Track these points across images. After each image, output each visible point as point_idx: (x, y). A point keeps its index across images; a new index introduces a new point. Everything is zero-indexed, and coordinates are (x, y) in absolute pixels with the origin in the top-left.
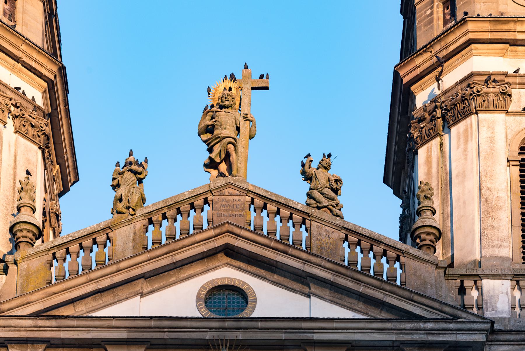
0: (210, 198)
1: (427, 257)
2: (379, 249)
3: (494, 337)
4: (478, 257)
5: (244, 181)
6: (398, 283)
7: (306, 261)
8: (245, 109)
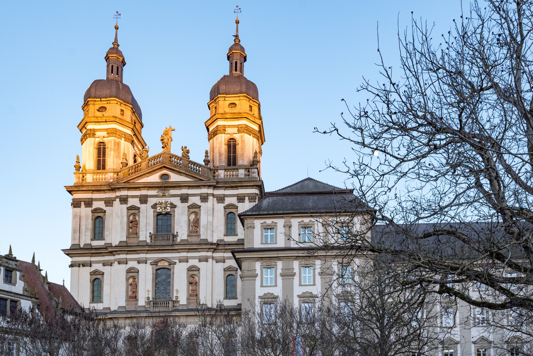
2: (196, 165)
8: (170, 135)
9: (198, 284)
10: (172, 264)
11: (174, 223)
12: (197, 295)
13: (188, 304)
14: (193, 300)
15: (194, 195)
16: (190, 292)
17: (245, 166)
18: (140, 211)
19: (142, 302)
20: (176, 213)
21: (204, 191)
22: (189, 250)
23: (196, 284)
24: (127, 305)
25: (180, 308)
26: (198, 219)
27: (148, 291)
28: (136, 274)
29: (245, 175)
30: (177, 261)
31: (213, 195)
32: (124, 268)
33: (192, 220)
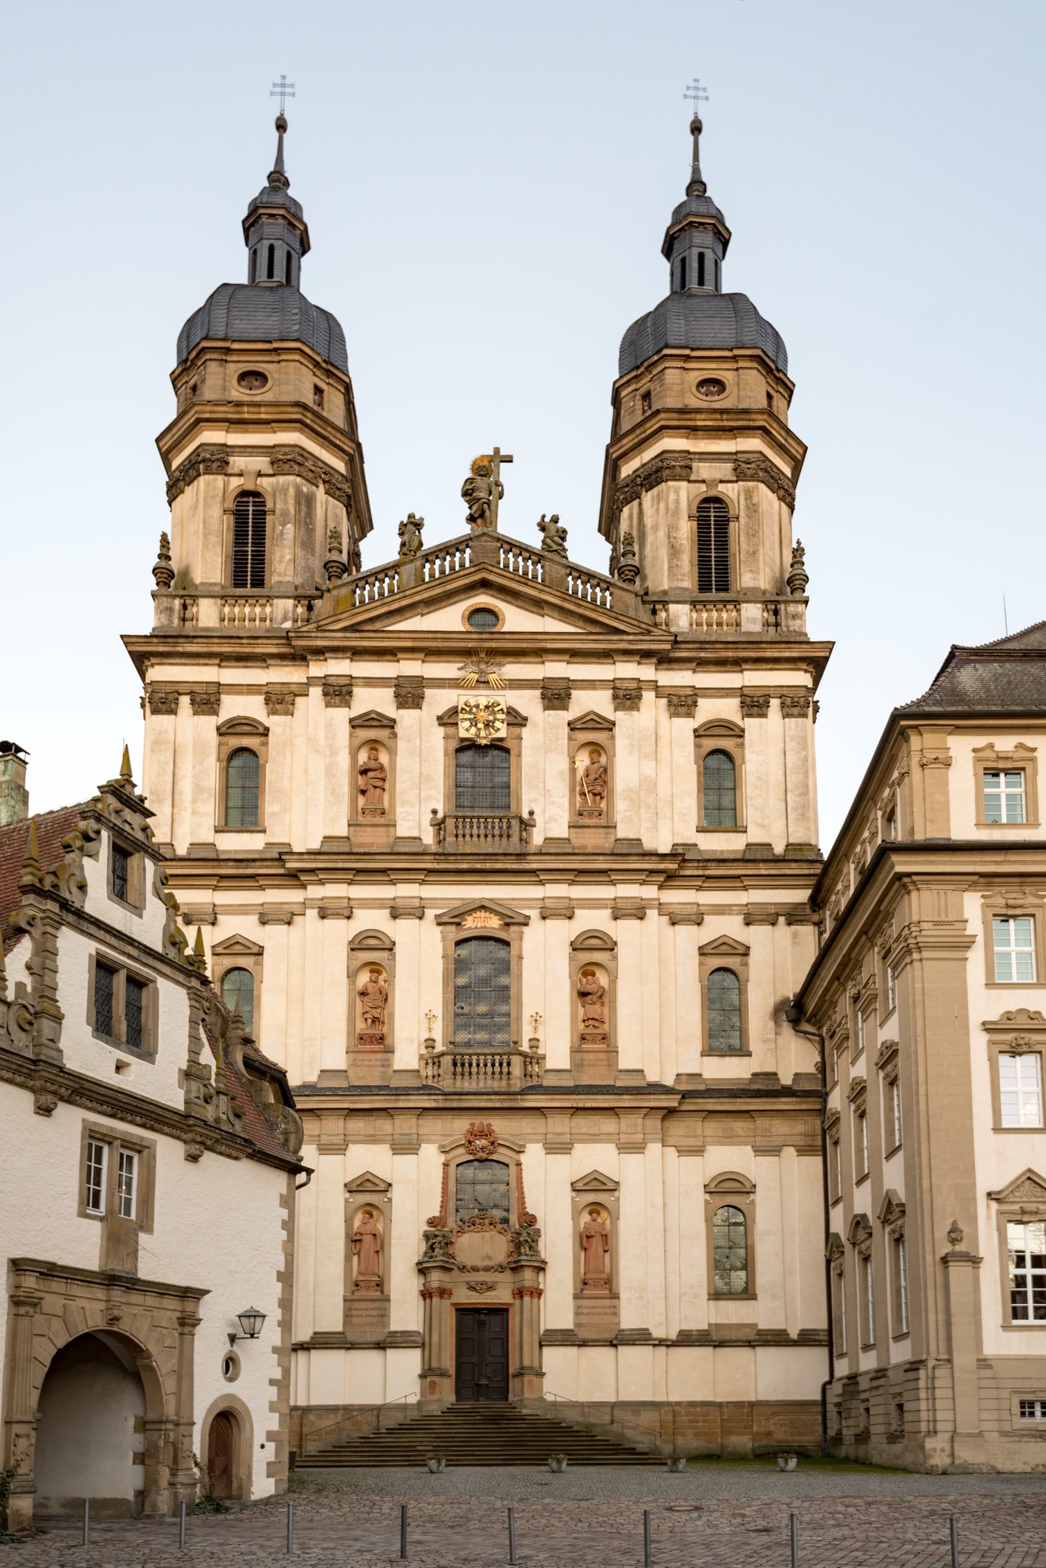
0: (470, 544)
1: (629, 588)
2: (594, 582)
3: (678, 646)
4: (666, 587)
5: (495, 531)
6: (608, 606)
7: (541, 591)
9: (606, 999)
10: (514, 921)
12: (604, 1038)
13: (578, 1065)
14: (592, 1056)
15: (591, 684)
16: (582, 1026)
17: (764, 592)
18: (395, 736)
20: (525, 743)
21: (627, 670)
22: (581, 876)
23: (601, 997)
24: (353, 1064)
25: (549, 1081)
26: (606, 770)
27: (430, 1018)
28: (386, 954)
29: (766, 624)
30: (534, 914)
31: (656, 687)
32: (342, 931)
33: (580, 772)
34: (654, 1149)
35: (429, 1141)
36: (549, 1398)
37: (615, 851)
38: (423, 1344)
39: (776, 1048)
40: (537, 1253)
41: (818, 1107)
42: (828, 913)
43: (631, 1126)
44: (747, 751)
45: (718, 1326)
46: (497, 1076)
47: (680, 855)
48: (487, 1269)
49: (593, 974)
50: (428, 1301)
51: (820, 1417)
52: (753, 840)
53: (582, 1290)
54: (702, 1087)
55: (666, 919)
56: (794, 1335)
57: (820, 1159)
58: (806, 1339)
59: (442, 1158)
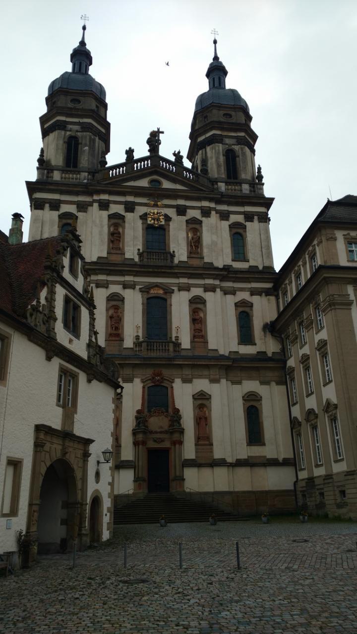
10: (169, 292)
11: (169, 239)
17: (249, 181)
18: (124, 222)
19: (129, 343)
20: (171, 227)
21: (205, 204)
24: (107, 345)
25: (183, 353)
26: (199, 238)
27: (138, 327)
28: (121, 303)
29: (251, 191)
30: (176, 289)
31: (214, 209)
34: (223, 381)
35: (137, 377)
36: (188, 490)
37: (205, 267)
38: (135, 466)
39: (265, 342)
40: (180, 425)
41: (282, 365)
42: (280, 292)
43: (214, 373)
44: (248, 234)
45: (251, 457)
46: (164, 351)
47: (227, 268)
48: (161, 432)
49: (197, 312)
50: (137, 447)
51: (294, 497)
52: (251, 265)
53: (198, 441)
54: (239, 357)
55: (222, 292)
56: (281, 460)
57: (285, 387)
58: (286, 463)
59: (141, 385)
